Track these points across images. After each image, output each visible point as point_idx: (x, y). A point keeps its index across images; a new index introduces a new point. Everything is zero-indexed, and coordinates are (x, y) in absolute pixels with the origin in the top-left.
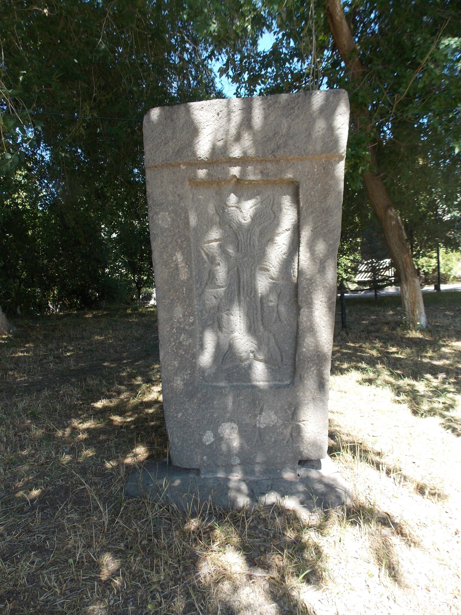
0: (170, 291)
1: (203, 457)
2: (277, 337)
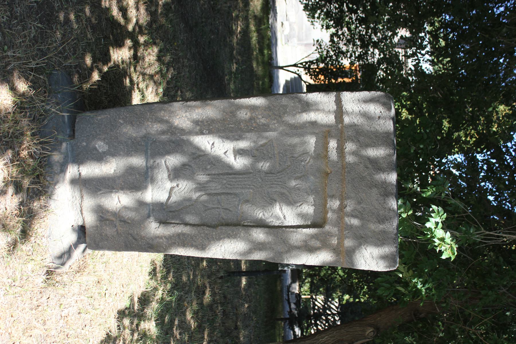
2: (191, 207)
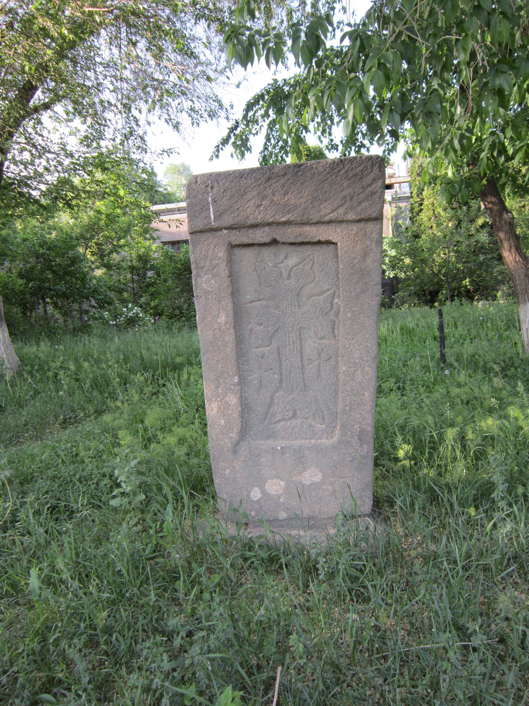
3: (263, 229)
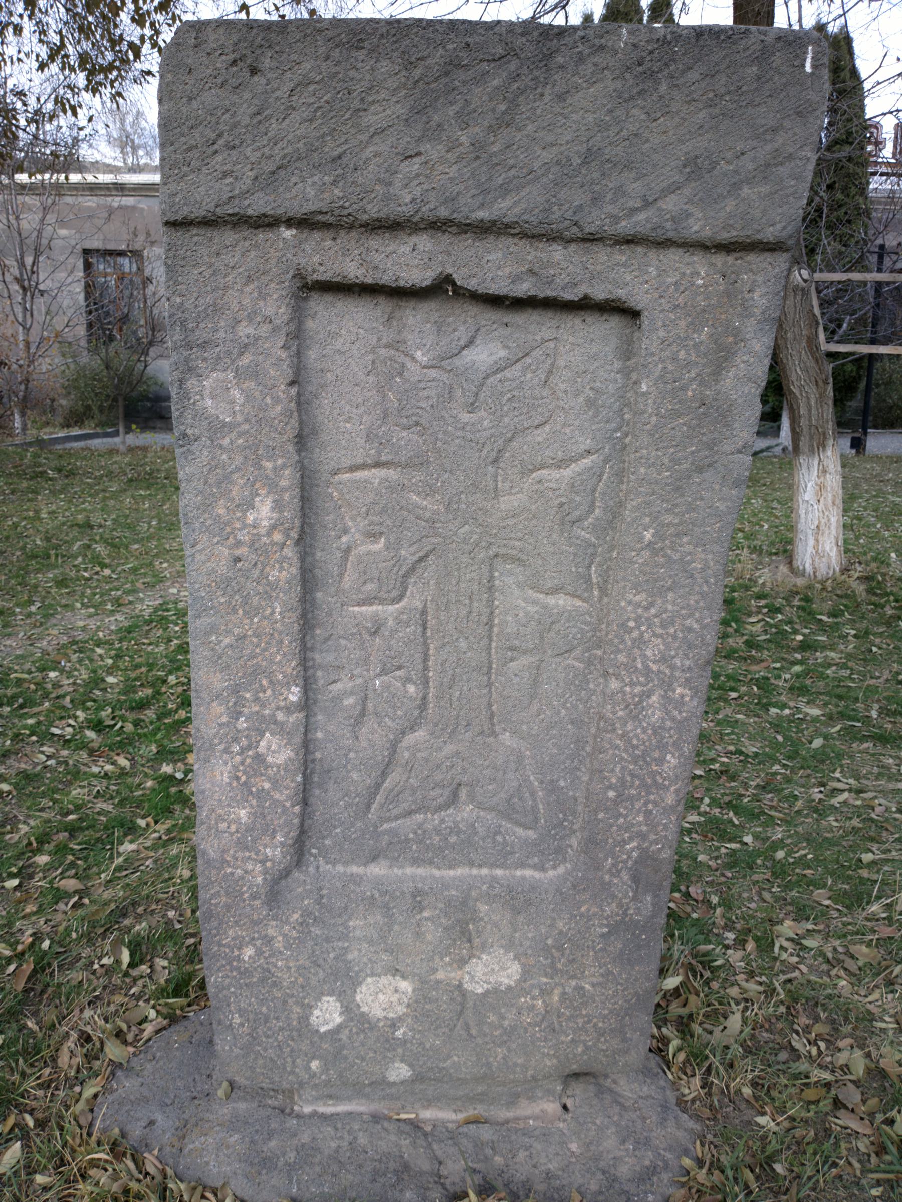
0: (235, 611)
1: (309, 1062)
3: (415, 239)
